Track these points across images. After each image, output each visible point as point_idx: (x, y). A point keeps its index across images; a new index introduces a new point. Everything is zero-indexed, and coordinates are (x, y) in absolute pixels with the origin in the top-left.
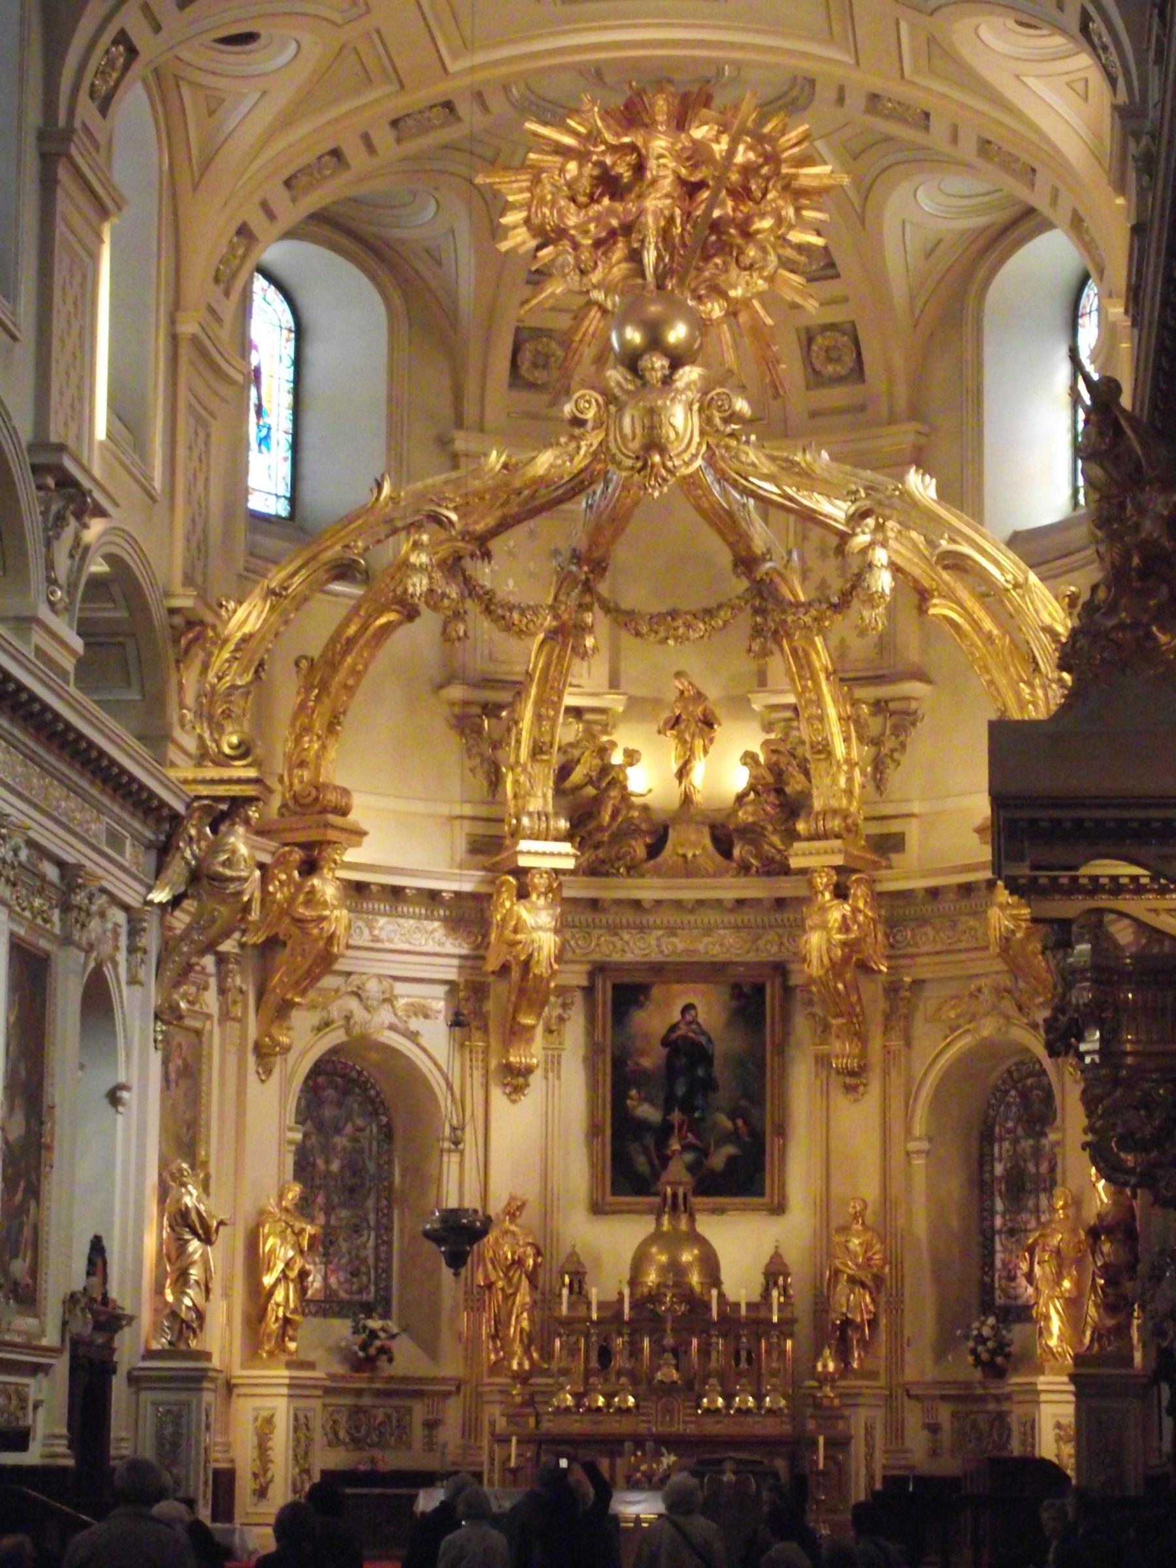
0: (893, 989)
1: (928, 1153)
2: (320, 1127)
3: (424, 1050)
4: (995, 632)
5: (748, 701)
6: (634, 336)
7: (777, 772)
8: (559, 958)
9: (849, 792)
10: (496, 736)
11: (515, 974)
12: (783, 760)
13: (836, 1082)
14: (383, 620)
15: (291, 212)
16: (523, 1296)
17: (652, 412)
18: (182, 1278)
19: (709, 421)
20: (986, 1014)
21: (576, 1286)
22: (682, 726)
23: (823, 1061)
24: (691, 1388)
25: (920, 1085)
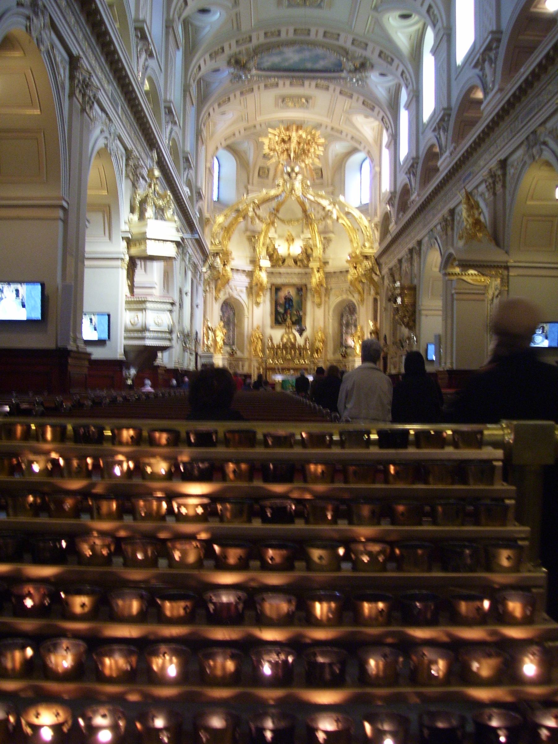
0: (326, 289)
4: (351, 226)
5: (300, 237)
6: (289, 169)
7: (306, 250)
9: (320, 254)
11: (259, 285)
15: (224, 144)
16: (260, 342)
17: (293, 182)
18: (208, 339)
19: (303, 186)
23: (313, 302)
24: (293, 360)
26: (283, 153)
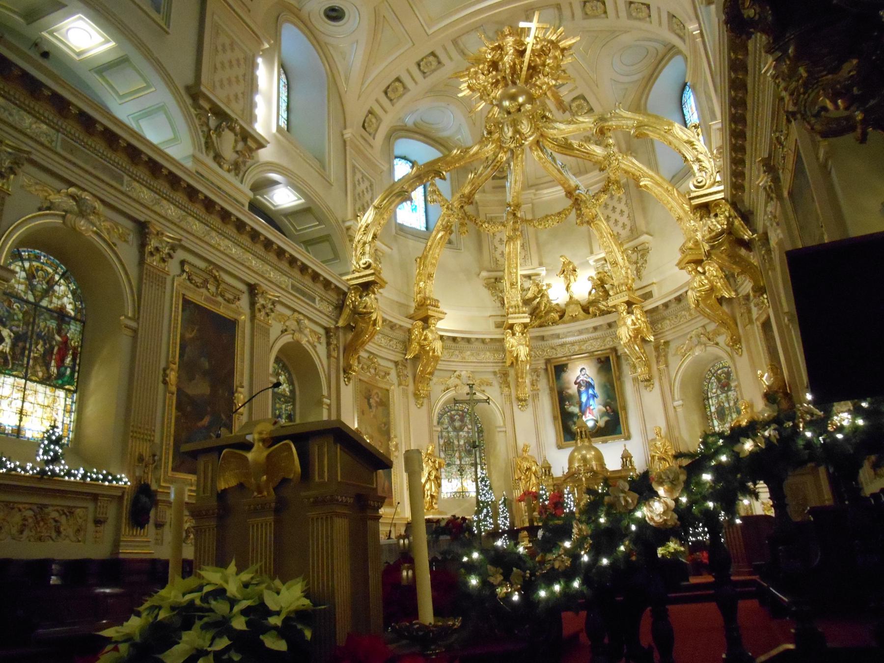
0: (657, 348)
1: (683, 405)
2: (455, 429)
5: (588, 261)
7: (601, 279)
8: (529, 355)
10: (501, 289)
11: (515, 361)
13: (642, 385)
14: (440, 235)
20: (696, 345)
21: (547, 472)
23: (635, 380)
25: (675, 380)
26: (496, 84)
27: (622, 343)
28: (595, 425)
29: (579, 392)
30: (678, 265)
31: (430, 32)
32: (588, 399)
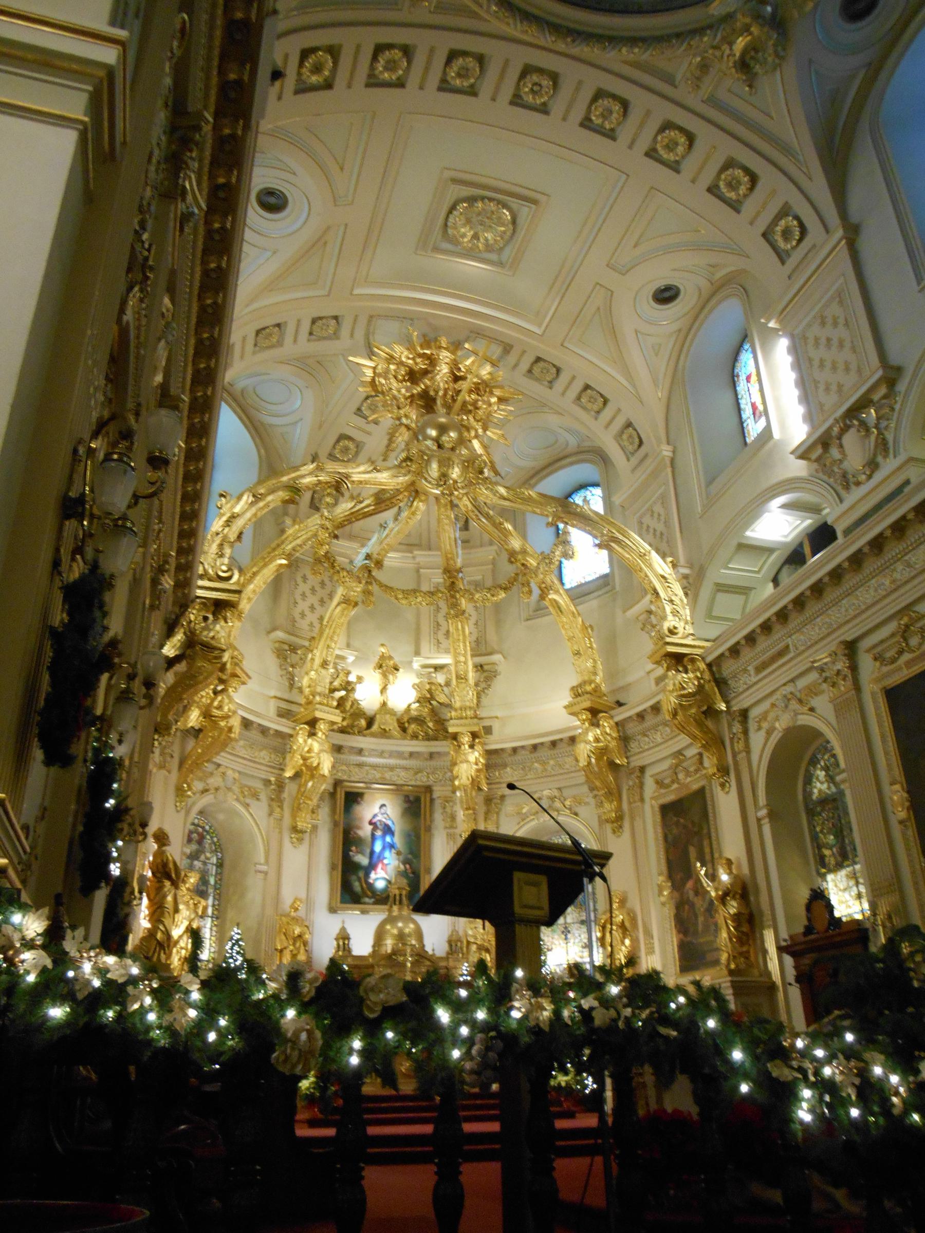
3: (252, 815)
5: (411, 662)
12: (433, 688)
22: (385, 669)
27: (457, 783)
28: (387, 888)
29: (373, 835)
30: (565, 707)
31: (356, 292)
32: (384, 848)
